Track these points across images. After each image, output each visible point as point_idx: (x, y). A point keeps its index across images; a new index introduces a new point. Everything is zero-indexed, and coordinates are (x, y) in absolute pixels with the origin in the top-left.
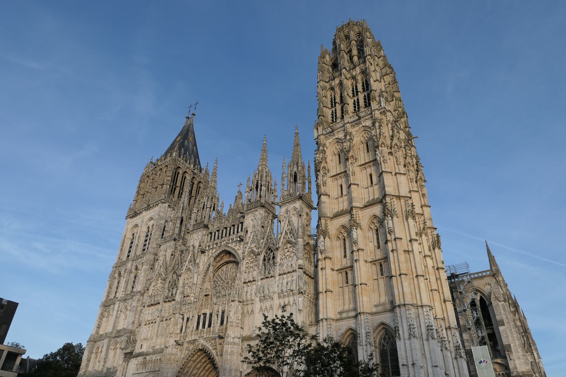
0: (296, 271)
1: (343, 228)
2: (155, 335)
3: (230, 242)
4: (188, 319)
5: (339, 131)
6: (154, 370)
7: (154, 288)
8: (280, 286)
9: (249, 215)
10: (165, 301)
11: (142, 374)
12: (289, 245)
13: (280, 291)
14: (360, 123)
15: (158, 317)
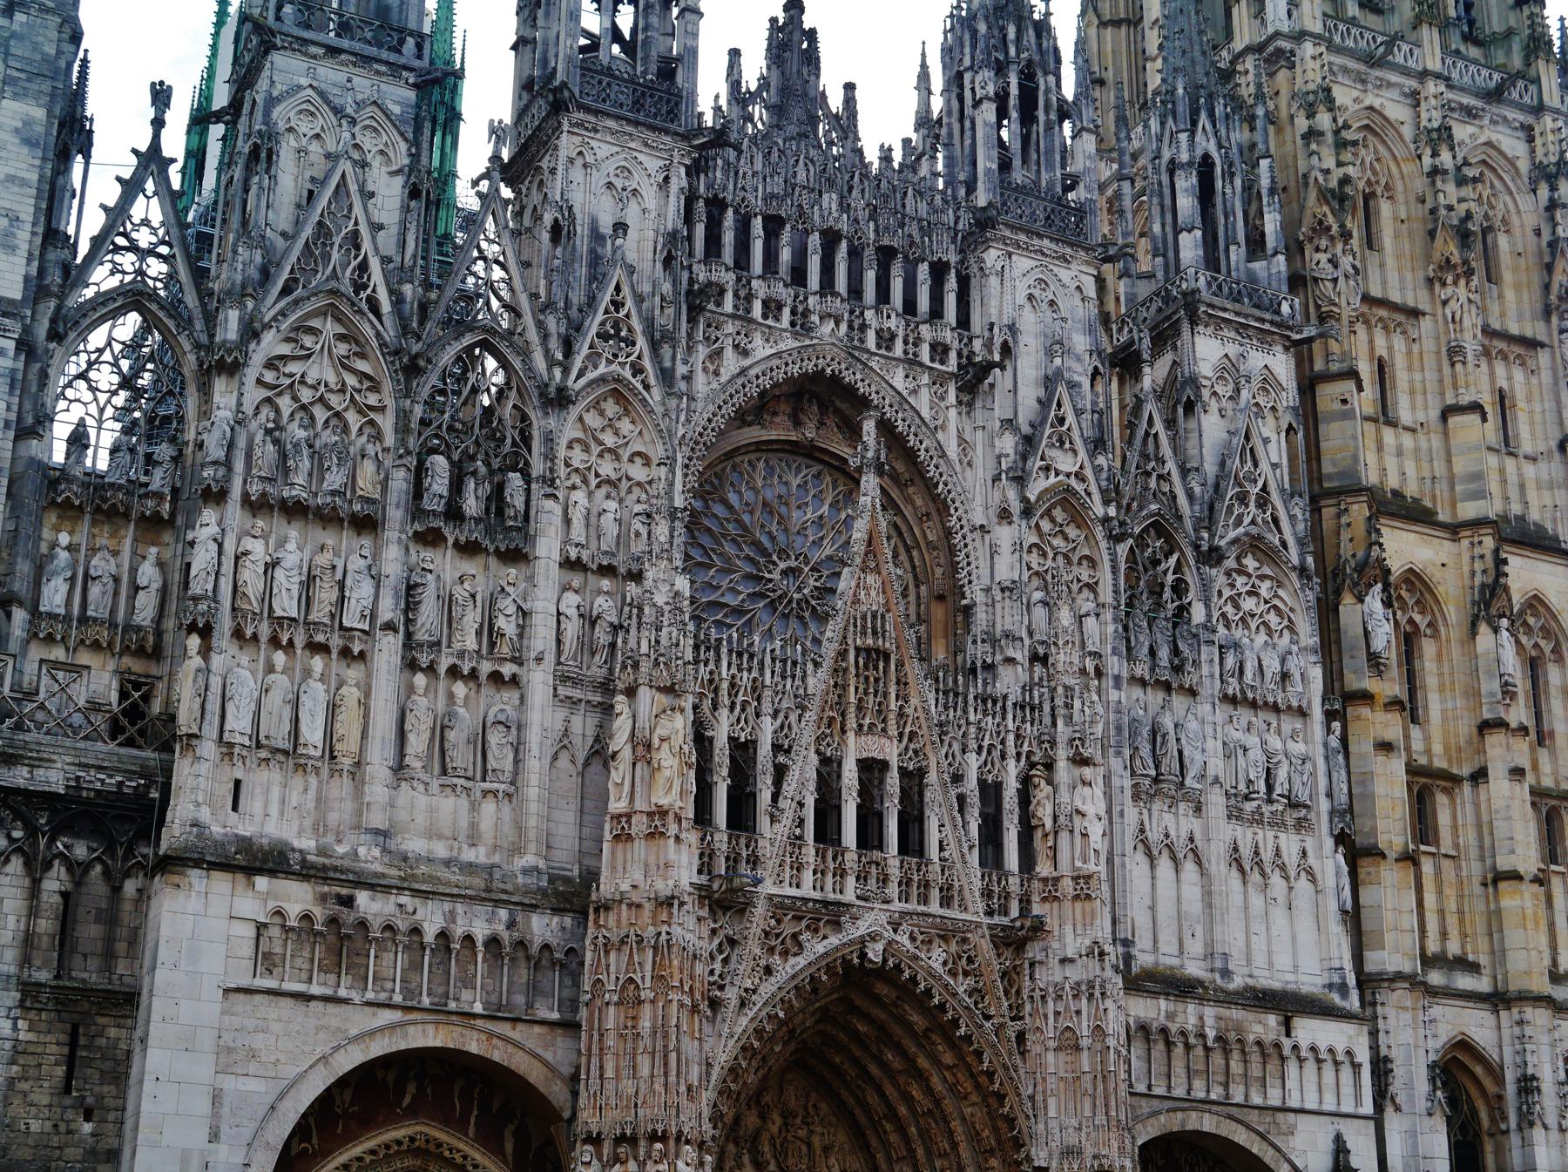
0: (1302, 713)
1: (1407, 581)
2: (391, 752)
3: (871, 342)
4: (743, 751)
5: (1390, 85)
6: (452, 1005)
7: (269, 377)
8: (1241, 761)
9: (1022, 263)
10: (430, 538)
11: (331, 1008)
12: (1250, 563)
13: (1242, 787)
14: (1475, 117)
15: (390, 627)
